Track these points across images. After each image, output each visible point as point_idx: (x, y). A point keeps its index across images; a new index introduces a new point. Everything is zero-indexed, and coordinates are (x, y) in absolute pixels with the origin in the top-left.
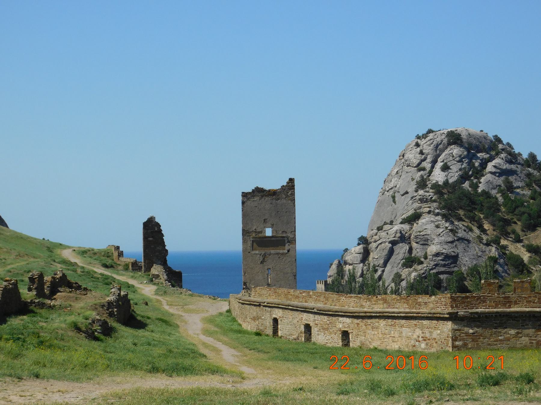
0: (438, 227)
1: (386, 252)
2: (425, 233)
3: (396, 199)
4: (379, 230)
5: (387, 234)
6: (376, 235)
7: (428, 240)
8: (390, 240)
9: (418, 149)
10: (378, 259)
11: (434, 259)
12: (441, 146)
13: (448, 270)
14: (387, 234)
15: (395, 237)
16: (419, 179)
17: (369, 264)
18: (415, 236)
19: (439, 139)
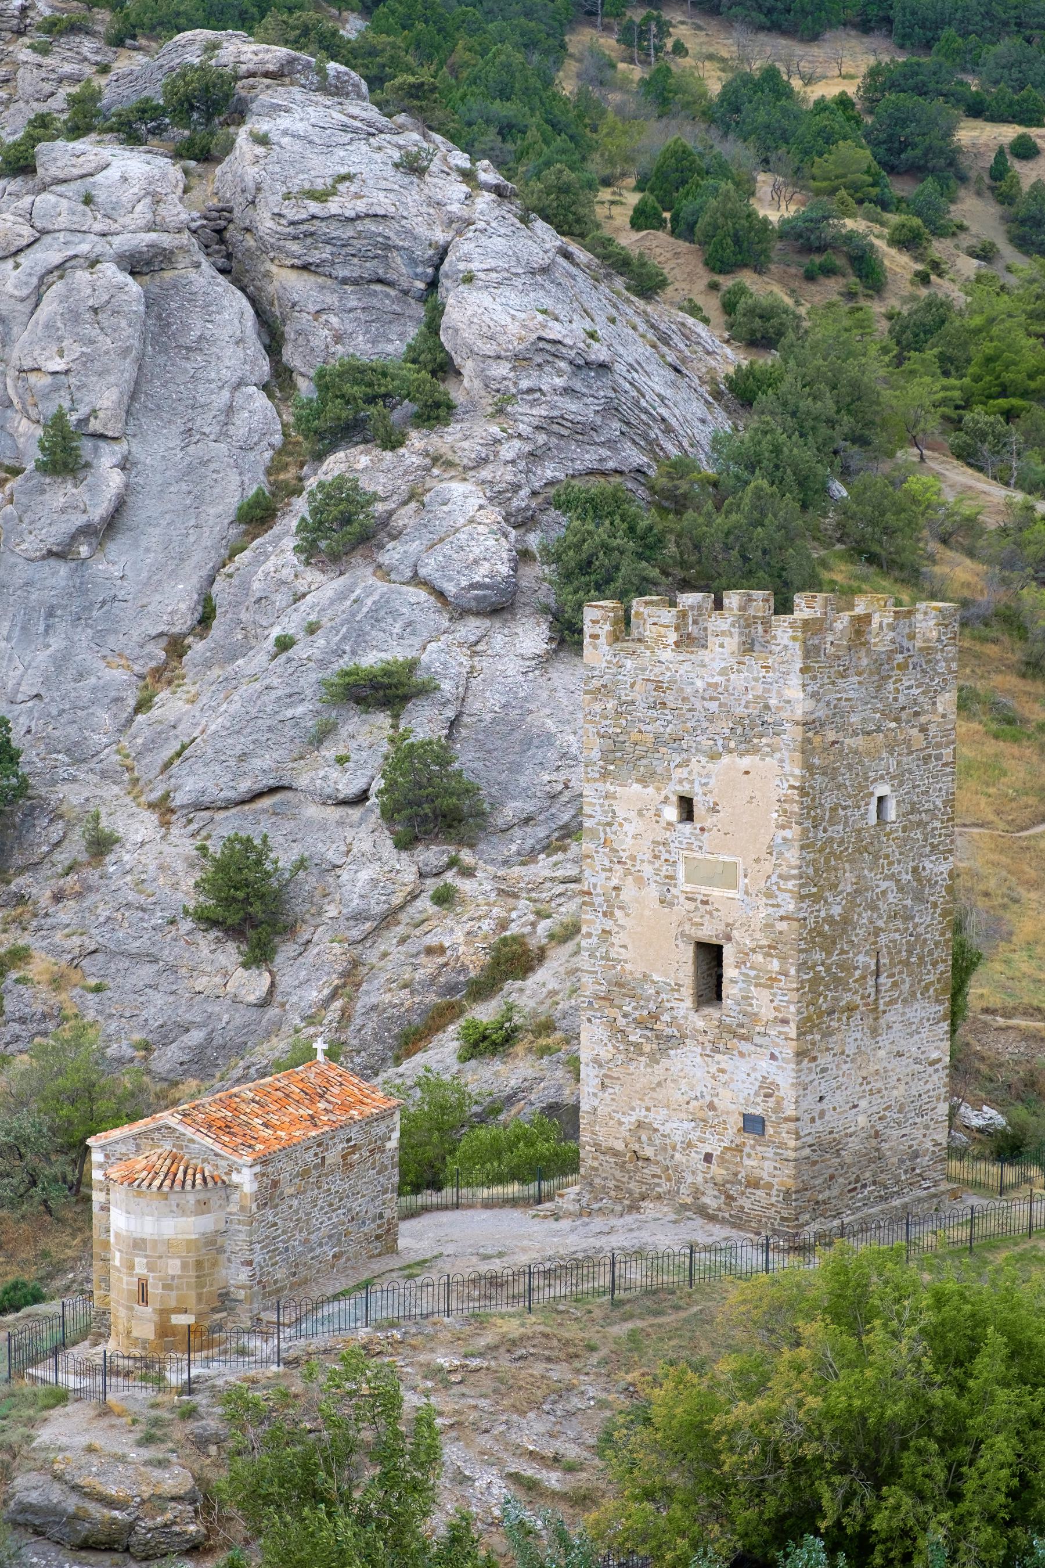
2: (361, 207)
5: (88, 200)
7: (387, 247)
8: (122, 242)
10: (73, 380)
11: (525, 384)
13: (611, 464)
18: (292, 223)
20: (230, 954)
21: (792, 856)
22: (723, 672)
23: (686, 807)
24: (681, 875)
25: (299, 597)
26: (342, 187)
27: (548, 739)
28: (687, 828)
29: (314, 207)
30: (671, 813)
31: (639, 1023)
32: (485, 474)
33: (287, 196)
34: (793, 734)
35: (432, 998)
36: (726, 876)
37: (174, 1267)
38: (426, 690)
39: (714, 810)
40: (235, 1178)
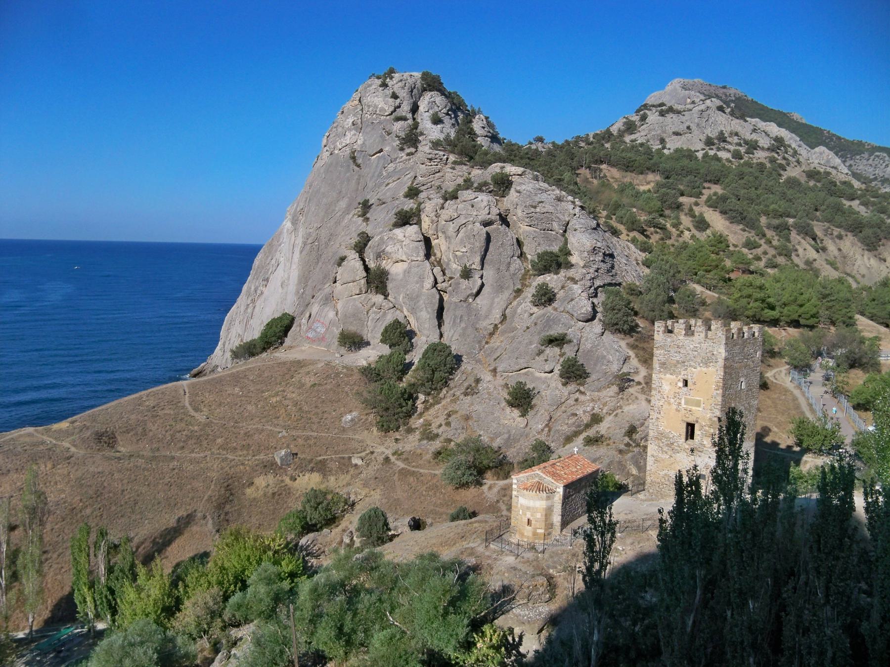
0: (559, 199)
1: (480, 243)
2: (545, 210)
3: (359, 161)
4: (446, 200)
6: (442, 208)
9: (389, 92)
10: (467, 254)
11: (592, 259)
12: (415, 91)
14: (473, 206)
15: (489, 214)
16: (403, 135)
17: (439, 263)
19: (411, 81)
20: (516, 413)
21: (720, 399)
22: (699, 343)
23: (686, 383)
24: (683, 402)
25: (532, 314)
26: (540, 205)
27: (604, 357)
28: (685, 389)
29: (533, 210)
30: (681, 384)
31: (667, 445)
32: (582, 282)
33: (525, 206)
34: (721, 362)
35: (574, 429)
36: (698, 404)
37: (539, 516)
38: (570, 341)
39: (694, 384)
40: (558, 490)
